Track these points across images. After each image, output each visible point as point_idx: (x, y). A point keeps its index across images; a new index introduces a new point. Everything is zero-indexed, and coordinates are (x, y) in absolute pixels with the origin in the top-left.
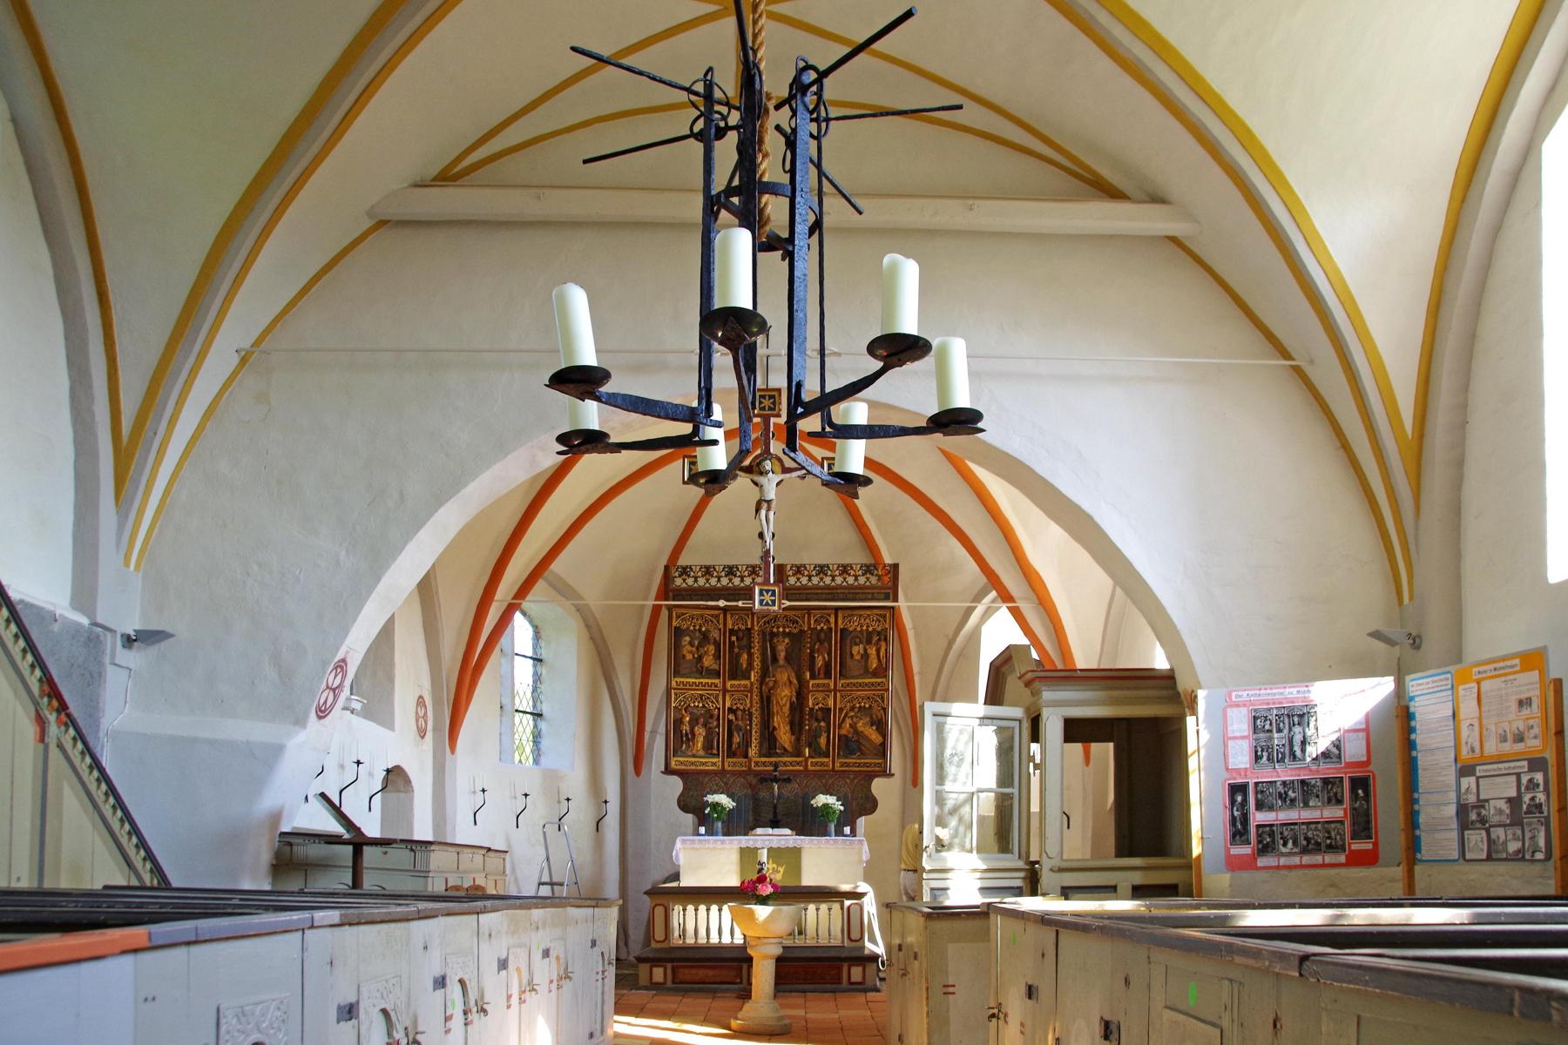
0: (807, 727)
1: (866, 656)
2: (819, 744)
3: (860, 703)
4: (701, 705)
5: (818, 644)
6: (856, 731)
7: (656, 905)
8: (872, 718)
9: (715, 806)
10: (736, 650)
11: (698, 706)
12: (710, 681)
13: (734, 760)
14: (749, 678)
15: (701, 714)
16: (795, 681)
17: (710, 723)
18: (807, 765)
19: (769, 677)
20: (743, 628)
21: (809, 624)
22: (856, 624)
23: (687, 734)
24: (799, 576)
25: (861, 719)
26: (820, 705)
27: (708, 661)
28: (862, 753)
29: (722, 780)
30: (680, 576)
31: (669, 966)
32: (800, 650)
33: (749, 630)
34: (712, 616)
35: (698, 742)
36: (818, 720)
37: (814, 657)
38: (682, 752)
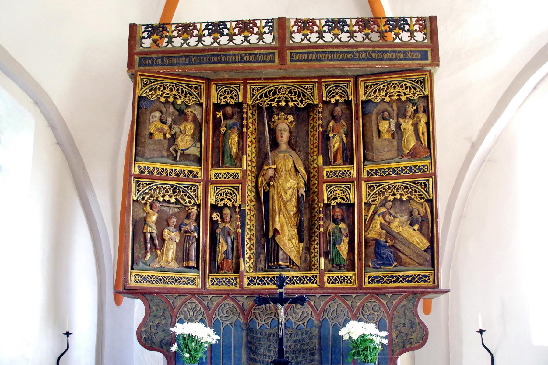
0: (322, 229)
4: (173, 200)
6: (390, 233)
8: (411, 215)
10: (223, 130)
12: (187, 169)
13: (220, 275)
14: (241, 166)
15: (174, 215)
16: (302, 170)
17: (186, 225)
19: (269, 164)
20: (232, 102)
24: (306, 32)
26: (339, 200)
28: (400, 263)
29: (200, 302)
33: (239, 105)
35: (168, 250)
36: (335, 221)
38: (145, 263)
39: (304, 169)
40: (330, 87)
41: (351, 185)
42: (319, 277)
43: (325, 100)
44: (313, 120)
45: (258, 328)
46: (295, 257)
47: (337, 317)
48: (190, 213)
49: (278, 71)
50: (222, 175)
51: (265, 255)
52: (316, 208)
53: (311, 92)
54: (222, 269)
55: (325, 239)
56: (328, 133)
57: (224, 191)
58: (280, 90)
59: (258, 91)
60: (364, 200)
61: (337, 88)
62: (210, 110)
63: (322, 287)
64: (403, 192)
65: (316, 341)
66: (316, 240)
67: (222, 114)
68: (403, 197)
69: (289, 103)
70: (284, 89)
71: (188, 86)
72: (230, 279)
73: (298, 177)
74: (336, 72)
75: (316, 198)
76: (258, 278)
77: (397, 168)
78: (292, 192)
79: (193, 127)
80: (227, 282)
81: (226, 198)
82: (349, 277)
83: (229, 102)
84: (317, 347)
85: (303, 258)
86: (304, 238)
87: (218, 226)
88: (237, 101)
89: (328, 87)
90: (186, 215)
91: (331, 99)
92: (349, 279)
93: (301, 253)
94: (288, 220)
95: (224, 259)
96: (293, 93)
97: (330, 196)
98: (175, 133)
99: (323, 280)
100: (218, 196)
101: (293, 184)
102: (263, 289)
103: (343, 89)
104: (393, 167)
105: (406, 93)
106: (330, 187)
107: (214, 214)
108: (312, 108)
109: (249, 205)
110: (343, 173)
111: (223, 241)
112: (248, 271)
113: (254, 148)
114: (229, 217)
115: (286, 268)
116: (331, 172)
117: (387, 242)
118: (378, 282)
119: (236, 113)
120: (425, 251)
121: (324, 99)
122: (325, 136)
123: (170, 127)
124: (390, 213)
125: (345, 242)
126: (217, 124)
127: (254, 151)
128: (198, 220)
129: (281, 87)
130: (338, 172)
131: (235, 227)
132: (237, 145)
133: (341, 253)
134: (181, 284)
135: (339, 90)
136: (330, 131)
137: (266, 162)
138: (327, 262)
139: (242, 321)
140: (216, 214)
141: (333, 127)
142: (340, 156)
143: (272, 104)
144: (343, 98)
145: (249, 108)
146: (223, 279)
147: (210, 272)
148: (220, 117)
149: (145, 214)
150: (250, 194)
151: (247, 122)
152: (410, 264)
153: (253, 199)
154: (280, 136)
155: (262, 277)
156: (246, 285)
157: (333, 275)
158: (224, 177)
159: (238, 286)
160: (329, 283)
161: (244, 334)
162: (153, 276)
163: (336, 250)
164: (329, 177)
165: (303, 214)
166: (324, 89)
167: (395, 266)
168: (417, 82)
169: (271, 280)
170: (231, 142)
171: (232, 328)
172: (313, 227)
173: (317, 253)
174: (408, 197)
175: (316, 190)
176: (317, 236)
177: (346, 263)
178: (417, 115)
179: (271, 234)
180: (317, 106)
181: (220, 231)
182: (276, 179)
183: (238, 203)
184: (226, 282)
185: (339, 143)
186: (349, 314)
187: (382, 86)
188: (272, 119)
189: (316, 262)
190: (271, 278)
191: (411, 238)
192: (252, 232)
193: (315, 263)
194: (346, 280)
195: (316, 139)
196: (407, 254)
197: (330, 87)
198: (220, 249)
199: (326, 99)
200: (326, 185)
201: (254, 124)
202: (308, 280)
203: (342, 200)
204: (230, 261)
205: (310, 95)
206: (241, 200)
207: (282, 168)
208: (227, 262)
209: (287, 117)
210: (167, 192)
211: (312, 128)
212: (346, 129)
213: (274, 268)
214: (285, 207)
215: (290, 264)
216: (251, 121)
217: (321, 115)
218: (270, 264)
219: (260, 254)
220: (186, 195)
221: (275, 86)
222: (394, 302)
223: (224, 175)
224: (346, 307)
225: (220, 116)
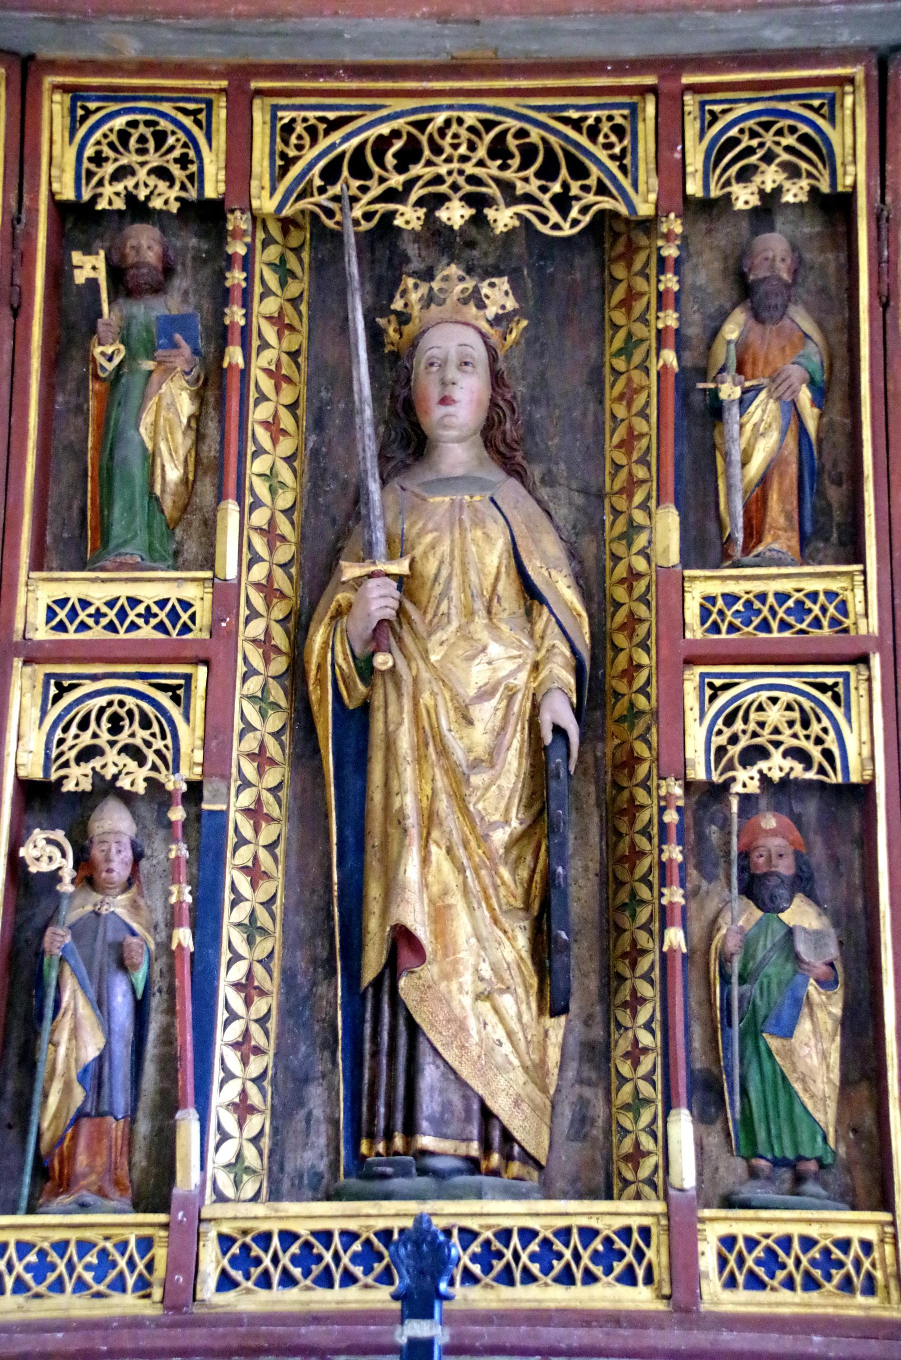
0: (675, 937)
14: (209, 561)
19: (368, 554)
39: (570, 581)
40: (730, 117)
41: (846, 676)
42: (664, 1238)
43: (700, 194)
44: (626, 304)
46: (517, 1104)
49: (431, 26)
50: (91, 610)
51: (332, 1089)
52: (642, 807)
53: (617, 150)
54: (65, 1184)
55: (697, 993)
56: (714, 380)
57: (102, 701)
58: (442, 134)
59: (314, 141)
61: (767, 126)
62: (31, 239)
63: (688, 1311)
66: (643, 1001)
67: (101, 264)
69: (490, 213)
70: (464, 134)
72: (109, 1245)
73: (539, 626)
74: (767, 33)
75: (641, 749)
76: (288, 1237)
78: (500, 714)
80: (88, 1267)
81: (112, 744)
82: (856, 1247)
83: (148, 198)
85: (567, 1113)
86: (575, 985)
87: (57, 909)
88: (192, 194)
89: (715, 118)
92: (858, 1264)
93: (553, 1081)
94: (478, 876)
95: (81, 1114)
96: (512, 156)
97: (722, 740)
99: (693, 1256)
100: (66, 730)
101: (510, 666)
102: (317, 1319)
103: (804, 129)
106: (726, 687)
107: (39, 835)
108: (623, 240)
109: (246, 784)
110: (800, 610)
111: (81, 1001)
112: (229, 1191)
113: (289, 460)
114: (128, 854)
115: (459, 1172)
116: (731, 599)
119: (189, 263)
121: (694, 188)
122: (697, 398)
125: (820, 1015)
127: (285, 474)
129: (448, 123)
130: (771, 600)
131: (160, 916)
132: (189, 442)
133: (797, 1087)
135: (780, 133)
136: (723, 369)
137: (354, 544)
138: (714, 1139)
140: (49, 841)
141: (743, 347)
142: (783, 510)
143: (392, 215)
144: (805, 183)
145: (260, 235)
146: (61, 1247)
148: (92, 283)
150: (254, 718)
151: (248, 316)
153: (273, 748)
154: (434, 392)
155: (314, 1234)
157: (754, 1230)
158: (104, 621)
159: (157, 1293)
160: (731, 1283)
163: (767, 1065)
164: (719, 631)
165: (563, 845)
166: (692, 129)
170: (155, 424)
172: (625, 921)
173: (654, 1084)
175: (642, 702)
176: (647, 977)
177: (835, 1153)
180: (648, 225)
181: (68, 939)
182: (408, 639)
183: (185, 772)
184: (79, 1269)
185: (773, 437)
188: (391, 299)
189: (647, 1143)
190: (368, 1243)
192: (264, 947)
193: (637, 1144)
194: (840, 1265)
195: (643, 414)
197: (730, 117)
198: (62, 1050)
199: (706, 186)
200: (703, 676)
201: (291, 328)
202: (596, 1257)
203: (799, 767)
204: (116, 1128)
205: (613, 166)
206: (199, 756)
207: (444, 573)
208: (99, 1135)
209: (476, 290)
211: (619, 353)
212: (816, 359)
213: (384, 1176)
214: (461, 801)
215: (487, 1147)
216: (271, 306)
217: (670, 281)
218: (364, 1148)
219: (306, 1080)
221: (415, 111)
223: (105, 609)
225: (92, 274)
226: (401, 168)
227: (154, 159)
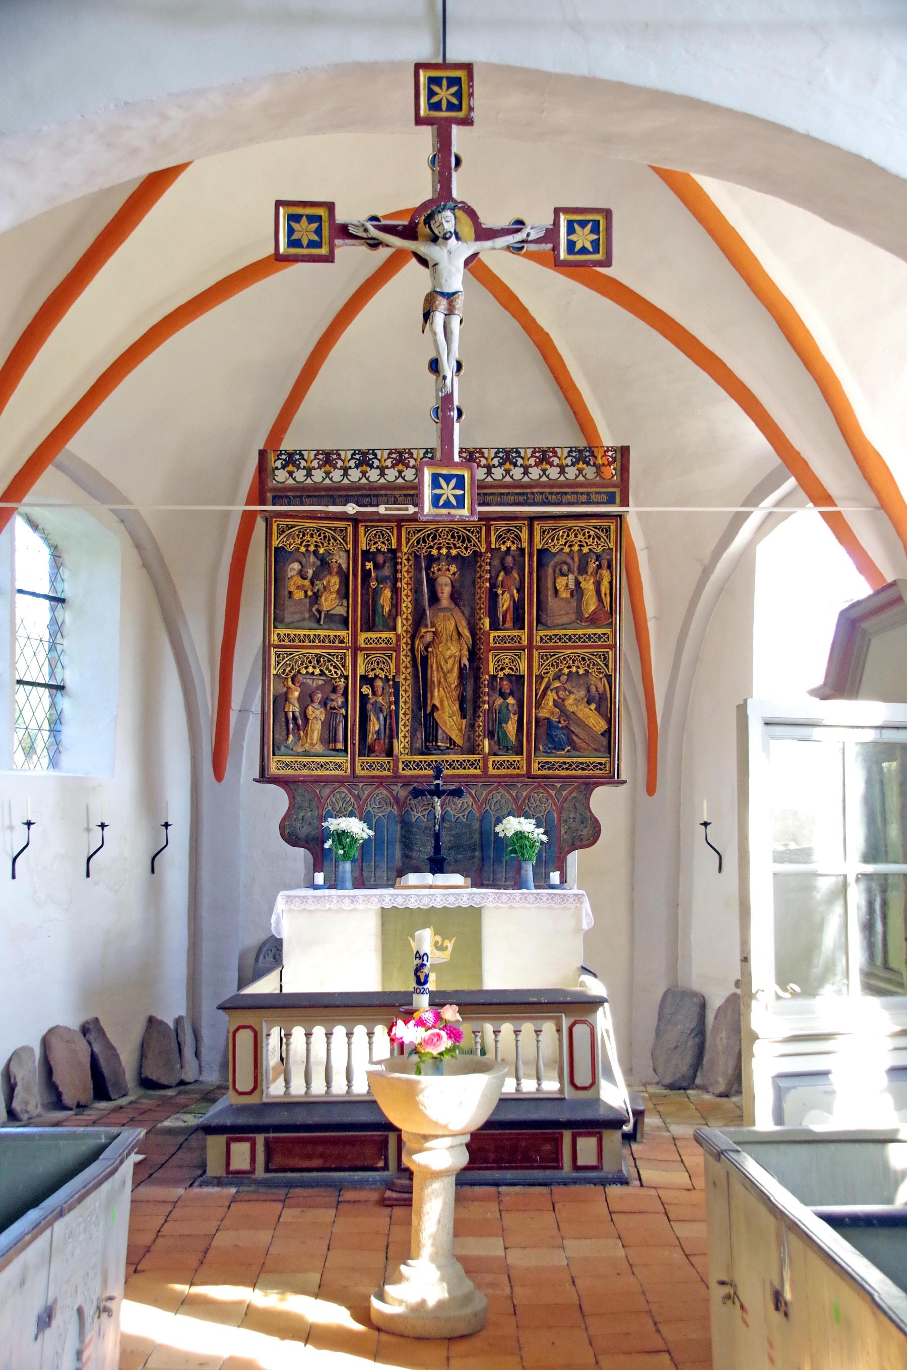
0: (486, 706)
1: (578, 592)
2: (505, 734)
3: (569, 667)
4: (317, 671)
5: (502, 574)
6: (563, 712)
7: (238, 1029)
8: (589, 691)
9: (341, 836)
10: (374, 584)
11: (313, 673)
12: (332, 633)
13: (370, 759)
14: (394, 629)
15: (319, 688)
16: (466, 633)
17: (333, 700)
18: (486, 767)
19: (426, 626)
20: (384, 548)
21: (488, 543)
22: (562, 541)
23: (295, 718)
25: (570, 692)
26: (507, 671)
27: (330, 603)
28: (575, 748)
30: (283, 467)
31: (260, 1139)
32: (474, 583)
33: (393, 552)
34: (335, 530)
35: (313, 732)
36: (502, 695)
37: (497, 595)
45: (414, 820)
47: (501, 808)
48: (337, 686)
54: (374, 752)
60: (536, 672)
64: (579, 665)
65: (477, 836)
68: (579, 670)
69: (451, 551)
71: (331, 530)
76: (414, 762)
77: (575, 635)
79: (338, 581)
84: (478, 842)
89: (498, 530)
90: (331, 688)
91: (502, 546)
98: (318, 590)
104: (570, 634)
105: (589, 543)
110: (512, 639)
116: (499, 637)
117: (559, 722)
118: (549, 769)
120: (602, 734)
121: (493, 546)
123: (312, 583)
124: (564, 687)
126: (366, 574)
128: (345, 694)
134: (328, 769)
138: (492, 743)
139: (396, 813)
141: (502, 581)
143: (431, 552)
146: (374, 763)
147: (359, 756)
148: (370, 569)
149: (285, 689)
152: (585, 749)
156: (400, 771)
157: (499, 759)
160: (494, 768)
161: (399, 828)
162: (296, 762)
166: (493, 532)
167: (568, 751)
168: (602, 531)
169: (429, 765)
171: (385, 821)
174: (585, 670)
178: (600, 571)
179: (429, 710)
183: (392, 674)
186: (514, 807)
187: (561, 533)
191: (586, 719)
196: (582, 737)
204: (382, 742)
205: (476, 541)
208: (379, 742)
210: (310, 662)
214: (446, 679)
215: (451, 745)
220: (331, 665)
222: (564, 793)
224: (510, 798)
226: (432, 541)
227: (382, 540)
